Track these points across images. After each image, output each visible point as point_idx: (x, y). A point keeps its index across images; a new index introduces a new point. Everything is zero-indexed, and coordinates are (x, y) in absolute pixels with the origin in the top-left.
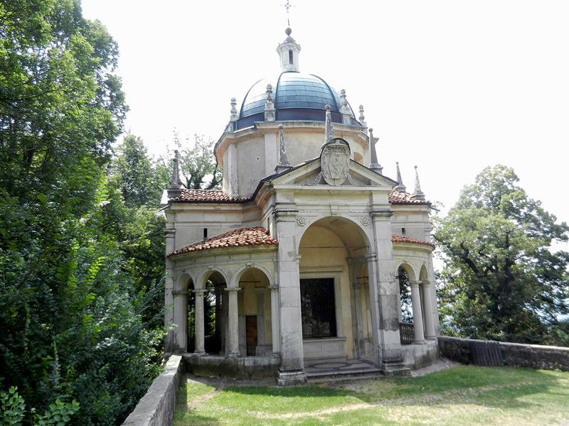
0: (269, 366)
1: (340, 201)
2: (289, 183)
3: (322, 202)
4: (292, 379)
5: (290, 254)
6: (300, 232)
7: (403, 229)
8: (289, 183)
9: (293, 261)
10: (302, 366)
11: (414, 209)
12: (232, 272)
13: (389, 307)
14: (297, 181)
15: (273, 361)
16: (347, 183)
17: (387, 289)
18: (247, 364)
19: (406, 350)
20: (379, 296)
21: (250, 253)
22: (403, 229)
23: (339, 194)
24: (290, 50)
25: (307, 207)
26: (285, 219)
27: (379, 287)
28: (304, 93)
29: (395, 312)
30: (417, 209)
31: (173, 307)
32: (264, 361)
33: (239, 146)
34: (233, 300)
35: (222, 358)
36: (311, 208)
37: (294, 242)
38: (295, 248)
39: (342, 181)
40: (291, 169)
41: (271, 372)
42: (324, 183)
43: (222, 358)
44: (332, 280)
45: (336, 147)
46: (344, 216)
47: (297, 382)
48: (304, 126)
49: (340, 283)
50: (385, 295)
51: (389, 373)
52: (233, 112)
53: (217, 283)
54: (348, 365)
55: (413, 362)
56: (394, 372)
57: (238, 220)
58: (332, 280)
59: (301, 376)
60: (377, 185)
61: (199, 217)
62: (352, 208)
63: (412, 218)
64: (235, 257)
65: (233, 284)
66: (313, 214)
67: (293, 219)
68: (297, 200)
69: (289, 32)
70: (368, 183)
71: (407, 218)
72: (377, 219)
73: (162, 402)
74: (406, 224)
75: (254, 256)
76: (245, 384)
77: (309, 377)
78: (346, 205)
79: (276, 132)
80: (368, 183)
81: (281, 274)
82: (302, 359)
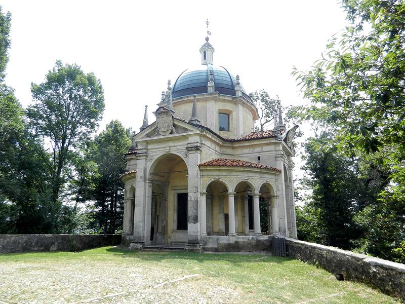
1: (172, 144)
2: (141, 138)
4: (135, 247)
5: (141, 177)
6: (150, 165)
7: (259, 158)
8: (141, 138)
9: (143, 181)
11: (265, 142)
17: (191, 196)
23: (170, 140)
24: (207, 50)
25: (154, 150)
26: (140, 158)
29: (196, 211)
36: (156, 150)
46: (173, 153)
50: (191, 200)
51: (186, 250)
56: (189, 250)
60: (193, 131)
62: (179, 147)
63: (266, 148)
66: (158, 153)
67: (144, 157)
68: (150, 147)
69: (207, 39)
70: (187, 130)
71: (262, 149)
72: (190, 152)
74: (260, 153)
78: (174, 146)
80: (187, 130)
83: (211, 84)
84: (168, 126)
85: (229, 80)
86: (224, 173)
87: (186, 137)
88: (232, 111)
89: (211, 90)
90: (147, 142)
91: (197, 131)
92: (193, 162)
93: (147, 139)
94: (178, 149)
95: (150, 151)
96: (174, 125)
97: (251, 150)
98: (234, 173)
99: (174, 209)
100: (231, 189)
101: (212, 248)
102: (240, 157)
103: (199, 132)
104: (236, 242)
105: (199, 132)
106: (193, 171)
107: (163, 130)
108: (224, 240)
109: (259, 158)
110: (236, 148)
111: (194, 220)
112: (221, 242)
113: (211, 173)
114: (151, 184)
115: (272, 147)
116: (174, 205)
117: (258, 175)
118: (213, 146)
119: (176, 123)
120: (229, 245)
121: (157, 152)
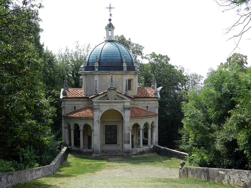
0: (91, 152)
1: (114, 104)
2: (97, 100)
3: (108, 105)
4: (96, 156)
5: (97, 121)
6: (101, 114)
8: (97, 100)
10: (100, 152)
12: (81, 125)
13: (127, 137)
14: (99, 99)
15: (92, 151)
16: (115, 99)
18: (85, 151)
19: (133, 150)
20: (125, 134)
21: (86, 119)
22: (147, 107)
27: (125, 131)
28: (109, 58)
29: (128, 139)
30: (153, 99)
31: (65, 132)
32: (89, 150)
33: (87, 76)
34: (81, 133)
35: (78, 149)
37: (99, 117)
38: (99, 119)
40: (98, 95)
41: (91, 153)
43: (78, 149)
44: (116, 126)
45: (111, 89)
46: (115, 109)
47: (97, 157)
48: (108, 73)
49: (119, 127)
51: (124, 156)
53: (77, 126)
54: (117, 153)
55: (136, 153)
57: (86, 103)
58: (116, 126)
59: (98, 155)
61: (73, 103)
63: (151, 102)
64: (82, 120)
65: (81, 128)
67: (98, 110)
68: (100, 104)
69: (110, 20)
70: (124, 99)
72: (125, 110)
73: (60, 158)
75: (87, 120)
76: (84, 156)
77: (101, 156)
79: (99, 74)
80: (124, 99)
81: (94, 127)
82: (100, 151)
83: (125, 65)
84: (114, 96)
85: (131, 59)
86: (139, 120)
88: (133, 79)
89: (125, 69)
90: (100, 102)
91: (129, 100)
92: (127, 115)
94: (118, 107)
96: (117, 95)
97: (143, 102)
98: (143, 119)
99: (103, 134)
101: (134, 154)
102: (137, 105)
103: (130, 101)
104: (143, 150)
105: (130, 101)
107: (111, 97)
108: (139, 150)
109: (147, 107)
110: (136, 100)
111: (128, 143)
112: (138, 151)
113: (134, 120)
115: (154, 102)
116: (103, 132)
117: (151, 118)
119: (118, 94)
120: (141, 152)
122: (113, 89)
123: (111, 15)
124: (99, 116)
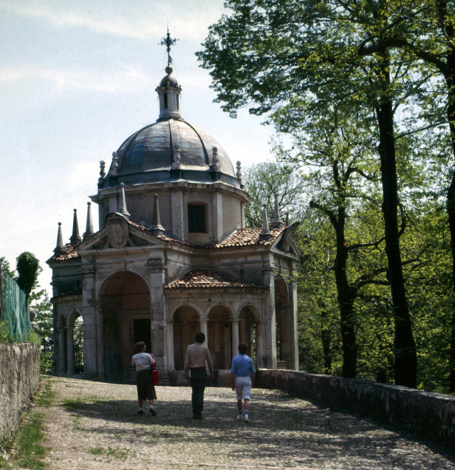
1: (128, 259)
2: (87, 249)
6: (99, 284)
8: (87, 249)
14: (94, 247)
16: (128, 245)
39: (125, 244)
42: (110, 246)
46: (131, 270)
52: (102, 173)
67: (92, 275)
68: (98, 261)
87: (146, 252)
93: (94, 251)
95: (100, 266)
96: (131, 235)
100: (204, 315)
106: (156, 296)
114: (101, 310)
118: (181, 259)
121: (109, 267)
122: (116, 220)
123: (170, 60)
124: (93, 290)
